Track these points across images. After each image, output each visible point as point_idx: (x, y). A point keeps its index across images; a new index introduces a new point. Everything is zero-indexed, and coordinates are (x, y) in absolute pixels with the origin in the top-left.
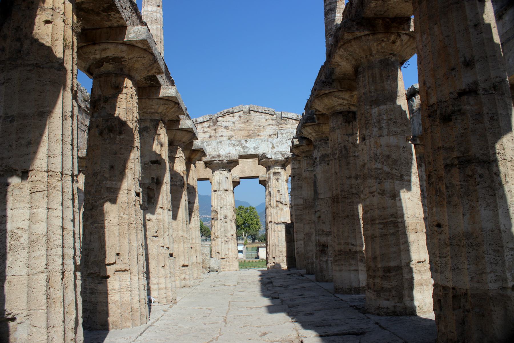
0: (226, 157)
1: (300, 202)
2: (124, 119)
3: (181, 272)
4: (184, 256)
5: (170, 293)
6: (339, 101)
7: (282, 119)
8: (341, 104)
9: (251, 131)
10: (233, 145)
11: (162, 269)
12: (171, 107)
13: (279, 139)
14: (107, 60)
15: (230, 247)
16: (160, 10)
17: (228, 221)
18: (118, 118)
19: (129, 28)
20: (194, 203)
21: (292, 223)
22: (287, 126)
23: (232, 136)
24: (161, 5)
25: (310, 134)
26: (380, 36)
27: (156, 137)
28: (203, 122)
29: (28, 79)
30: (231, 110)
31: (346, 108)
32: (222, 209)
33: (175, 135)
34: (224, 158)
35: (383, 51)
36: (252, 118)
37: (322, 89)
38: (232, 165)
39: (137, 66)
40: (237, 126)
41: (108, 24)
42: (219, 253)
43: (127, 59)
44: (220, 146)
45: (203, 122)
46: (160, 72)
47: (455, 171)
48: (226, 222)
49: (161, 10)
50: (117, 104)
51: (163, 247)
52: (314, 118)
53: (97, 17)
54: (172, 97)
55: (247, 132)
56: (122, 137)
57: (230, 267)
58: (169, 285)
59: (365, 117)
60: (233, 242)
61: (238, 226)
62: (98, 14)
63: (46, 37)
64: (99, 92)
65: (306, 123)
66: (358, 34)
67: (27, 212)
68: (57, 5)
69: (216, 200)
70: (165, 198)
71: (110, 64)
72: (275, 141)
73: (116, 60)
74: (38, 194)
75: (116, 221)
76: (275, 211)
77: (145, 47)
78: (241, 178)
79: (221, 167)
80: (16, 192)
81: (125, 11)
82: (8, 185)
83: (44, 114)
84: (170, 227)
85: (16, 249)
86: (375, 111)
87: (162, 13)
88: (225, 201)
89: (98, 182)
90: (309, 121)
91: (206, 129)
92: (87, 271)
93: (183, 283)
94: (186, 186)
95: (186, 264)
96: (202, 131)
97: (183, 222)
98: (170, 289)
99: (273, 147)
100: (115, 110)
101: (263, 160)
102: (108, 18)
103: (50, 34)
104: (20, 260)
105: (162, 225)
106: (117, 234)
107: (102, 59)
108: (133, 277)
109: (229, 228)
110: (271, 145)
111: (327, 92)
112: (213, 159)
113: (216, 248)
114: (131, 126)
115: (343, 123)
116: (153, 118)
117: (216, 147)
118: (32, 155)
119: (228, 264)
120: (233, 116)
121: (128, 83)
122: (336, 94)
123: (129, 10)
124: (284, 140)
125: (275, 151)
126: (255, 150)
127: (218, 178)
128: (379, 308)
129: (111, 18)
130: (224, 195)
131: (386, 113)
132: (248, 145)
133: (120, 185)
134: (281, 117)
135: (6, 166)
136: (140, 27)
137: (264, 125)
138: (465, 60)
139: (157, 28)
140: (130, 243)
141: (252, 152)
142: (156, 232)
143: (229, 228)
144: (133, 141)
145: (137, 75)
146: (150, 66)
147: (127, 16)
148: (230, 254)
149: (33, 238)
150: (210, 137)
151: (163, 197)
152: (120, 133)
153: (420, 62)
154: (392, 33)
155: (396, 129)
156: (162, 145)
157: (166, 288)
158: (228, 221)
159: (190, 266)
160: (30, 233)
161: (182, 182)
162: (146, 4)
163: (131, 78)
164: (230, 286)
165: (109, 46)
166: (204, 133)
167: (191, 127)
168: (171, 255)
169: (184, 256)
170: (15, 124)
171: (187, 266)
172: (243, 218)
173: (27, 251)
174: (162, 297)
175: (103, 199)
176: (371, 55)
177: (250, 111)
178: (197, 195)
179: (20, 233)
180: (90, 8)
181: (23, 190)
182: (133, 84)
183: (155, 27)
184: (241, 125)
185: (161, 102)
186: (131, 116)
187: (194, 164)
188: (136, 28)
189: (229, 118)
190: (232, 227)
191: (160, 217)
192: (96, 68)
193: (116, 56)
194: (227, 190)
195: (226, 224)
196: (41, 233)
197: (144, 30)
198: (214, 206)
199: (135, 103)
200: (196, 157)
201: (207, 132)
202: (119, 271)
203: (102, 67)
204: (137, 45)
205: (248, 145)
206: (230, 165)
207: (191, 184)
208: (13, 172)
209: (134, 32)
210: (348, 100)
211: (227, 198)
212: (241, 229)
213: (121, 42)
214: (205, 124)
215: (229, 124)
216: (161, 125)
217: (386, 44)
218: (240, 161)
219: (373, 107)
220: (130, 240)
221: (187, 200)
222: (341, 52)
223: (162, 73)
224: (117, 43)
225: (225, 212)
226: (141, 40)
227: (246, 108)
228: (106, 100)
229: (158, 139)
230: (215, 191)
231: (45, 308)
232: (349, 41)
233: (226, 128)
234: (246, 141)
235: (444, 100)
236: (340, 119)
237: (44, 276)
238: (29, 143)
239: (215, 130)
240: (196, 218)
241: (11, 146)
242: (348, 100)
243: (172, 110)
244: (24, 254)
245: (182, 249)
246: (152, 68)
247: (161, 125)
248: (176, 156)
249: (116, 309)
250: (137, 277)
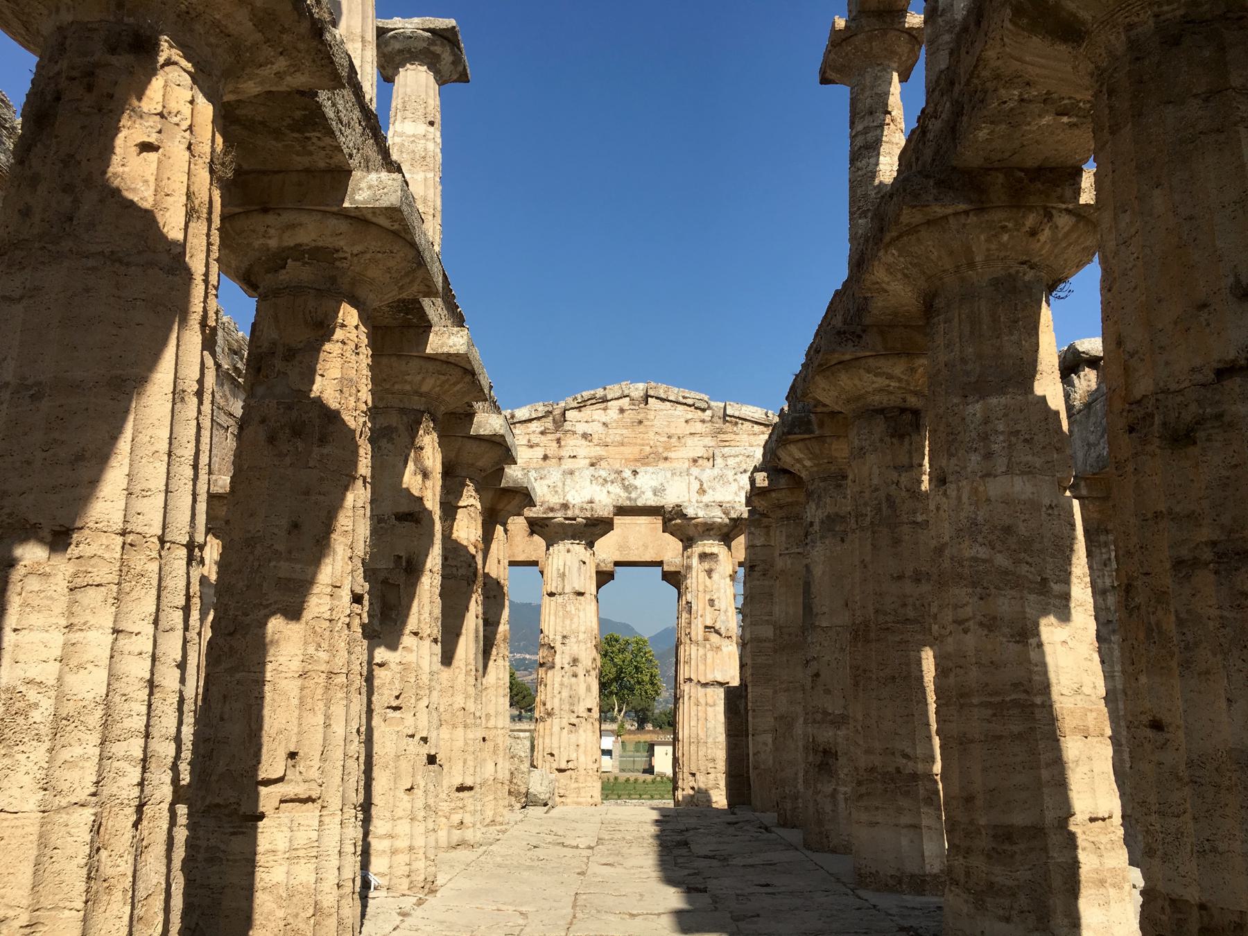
0: (582, 509)
1: (768, 632)
2: (334, 405)
3: (453, 805)
4: (465, 762)
5: (420, 864)
6: (879, 380)
7: (725, 421)
8: (881, 390)
9: (648, 448)
10: (601, 481)
11: (406, 797)
12: (453, 379)
13: (716, 471)
14: (298, 252)
15: (582, 742)
16: (435, 133)
17: (581, 672)
18: (318, 402)
19: (357, 174)
20: (498, 623)
21: (744, 684)
22: (737, 438)
23: (601, 459)
24: (438, 120)
25: (799, 461)
26: (997, 216)
27: (412, 454)
28: (530, 420)
29: (87, 290)
30: (600, 392)
31: (894, 400)
32: (567, 641)
33: (459, 449)
34: (577, 512)
35: (1002, 254)
36: (651, 415)
37: (834, 351)
38: (597, 530)
39: (374, 273)
40: (614, 435)
41: (304, 161)
42: (552, 755)
43: (348, 255)
44: (568, 481)
45: (530, 420)
46: (431, 292)
47: (1205, 579)
48: (575, 675)
49: (438, 134)
50: (319, 366)
51: (412, 736)
52: (809, 422)
53: (274, 143)
54: (457, 355)
55: (636, 449)
56: (325, 451)
57: (579, 794)
58: (419, 842)
59: (948, 425)
60: (589, 726)
61: (603, 686)
62: (277, 134)
63: (140, 185)
64: (270, 333)
65: (789, 433)
66: (938, 210)
67: (57, 639)
68: (173, 106)
69: (552, 618)
70: (427, 609)
71: (304, 264)
72: (708, 474)
73: (319, 255)
74: (91, 591)
75: (296, 665)
76: (701, 651)
77: (396, 227)
78: (617, 564)
79: (570, 534)
80: (33, 584)
81: (349, 131)
82: (12, 563)
83: (126, 384)
84: (433, 683)
85: (19, 737)
86: (976, 409)
87: (439, 140)
88: (575, 620)
89: (256, 564)
90: (796, 430)
91: (536, 439)
92: (204, 798)
93: (457, 835)
94: (480, 579)
95: (469, 783)
96: (525, 442)
97: (467, 673)
98: (422, 851)
99: (702, 491)
100: (313, 382)
101: (675, 521)
102: (304, 147)
103: (152, 179)
104: (23, 769)
105: (412, 680)
106: (296, 702)
107: (284, 249)
108: (326, 820)
109: (582, 690)
110: (696, 485)
111: (848, 357)
112: (551, 515)
113: (547, 740)
114: (352, 424)
115: (888, 439)
116: (407, 406)
117: (560, 484)
118: (84, 486)
119: (574, 785)
120: (605, 409)
121: (349, 315)
122: (871, 360)
123: (359, 129)
124: (730, 474)
126: (655, 494)
127: (561, 563)
129: (312, 148)
130: (573, 605)
131: (1005, 415)
132: (638, 482)
133: (314, 575)
134: (725, 415)
135: (10, 515)
136: (384, 175)
137: (679, 432)
138: (1238, 281)
139: (426, 179)
140: (327, 726)
141: (648, 499)
142: (397, 697)
143: (582, 690)
144: (354, 463)
145: (371, 296)
146: (407, 274)
147: (351, 145)
148: (582, 759)
149: (68, 708)
150: (545, 458)
151: (421, 607)
152: (323, 441)
154: (1031, 209)
155: (1029, 458)
156: (425, 475)
157: (411, 848)
158: (581, 672)
159: (477, 789)
160: (61, 697)
161: (472, 570)
162: (399, 114)
163: (355, 303)
164: (577, 847)
165: (304, 218)
166: (531, 447)
167: (502, 432)
168: (432, 760)
169: (465, 762)
171: (471, 788)
172: (615, 665)
173: (47, 745)
174: (400, 873)
175: (267, 606)
176: (971, 265)
177: (647, 397)
178: (507, 603)
179: (32, 695)
180: (259, 118)
181: (52, 579)
182: (360, 317)
183: (420, 176)
184: (624, 431)
185: (431, 366)
186: (352, 399)
187: (504, 524)
188: (373, 176)
189: (595, 413)
190: (589, 689)
191: (411, 658)
192: (267, 272)
193: (320, 244)
194: (581, 594)
195: (574, 679)
196: (90, 696)
197: (396, 184)
198: (546, 632)
199: (364, 365)
200: (509, 508)
201: (537, 445)
202: (292, 801)
203: (284, 271)
204: (374, 220)
205: (638, 482)
206: (592, 529)
207: (494, 575)
208: (28, 532)
209: (370, 187)
210: (900, 380)
211: (581, 614)
212: (611, 693)
213: (335, 209)
214: (535, 426)
215: (595, 429)
216: (427, 424)
217: (1011, 237)
218: (618, 521)
219: (970, 399)
220: (327, 717)
221: (481, 616)
222: (891, 256)
223: (436, 295)
224: (325, 212)
225: (573, 648)
226: (386, 208)
227: (637, 390)
228: (290, 354)
229: (418, 460)
230: (551, 594)
231: (81, 905)
232: (913, 230)
233: (585, 436)
234: (635, 473)
235: (1173, 387)
236: (879, 427)
237: (87, 815)
238: (79, 458)
239: (558, 441)
240: (500, 662)
241: (28, 463)
242: (900, 380)
243: (456, 389)
244: (39, 753)
245: (460, 743)
246: (412, 282)
247: (427, 424)
248: (461, 504)
249: (275, 906)
250: (338, 819)
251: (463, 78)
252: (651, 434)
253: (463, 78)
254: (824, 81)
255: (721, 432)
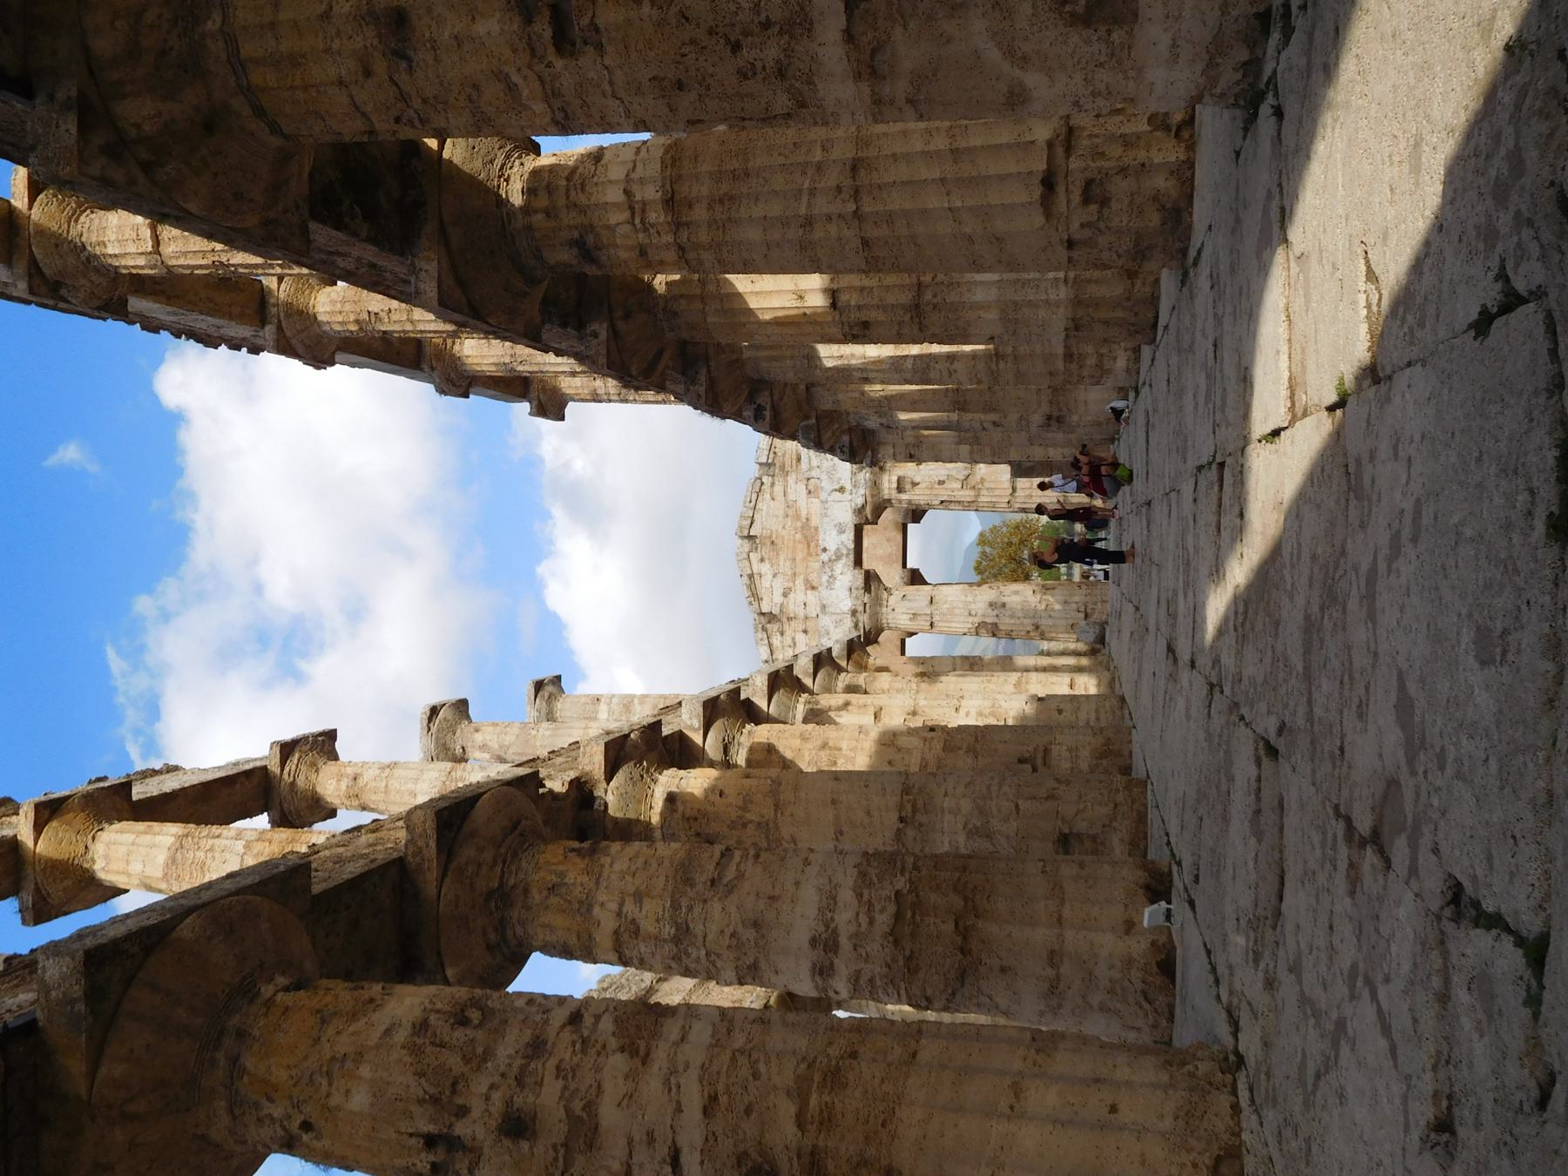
1: (965, 449)
13: (824, 477)
21: (1010, 463)
23: (807, 581)
40: (785, 566)
55: (800, 546)
72: (827, 485)
76: (984, 492)
91: (788, 640)
99: (842, 490)
125: (848, 486)
128: (1128, 371)
132: (832, 547)
148: (1076, 599)
150: (805, 632)
153: (747, 268)
170: (845, 829)
188: (684, 717)
189: (764, 584)
190: (1016, 593)
214: (776, 640)
234: (825, 550)
239: (789, 619)
251: (559, 678)
252: (784, 533)
253: (559, 678)
254: (562, 418)
255: (783, 467)
